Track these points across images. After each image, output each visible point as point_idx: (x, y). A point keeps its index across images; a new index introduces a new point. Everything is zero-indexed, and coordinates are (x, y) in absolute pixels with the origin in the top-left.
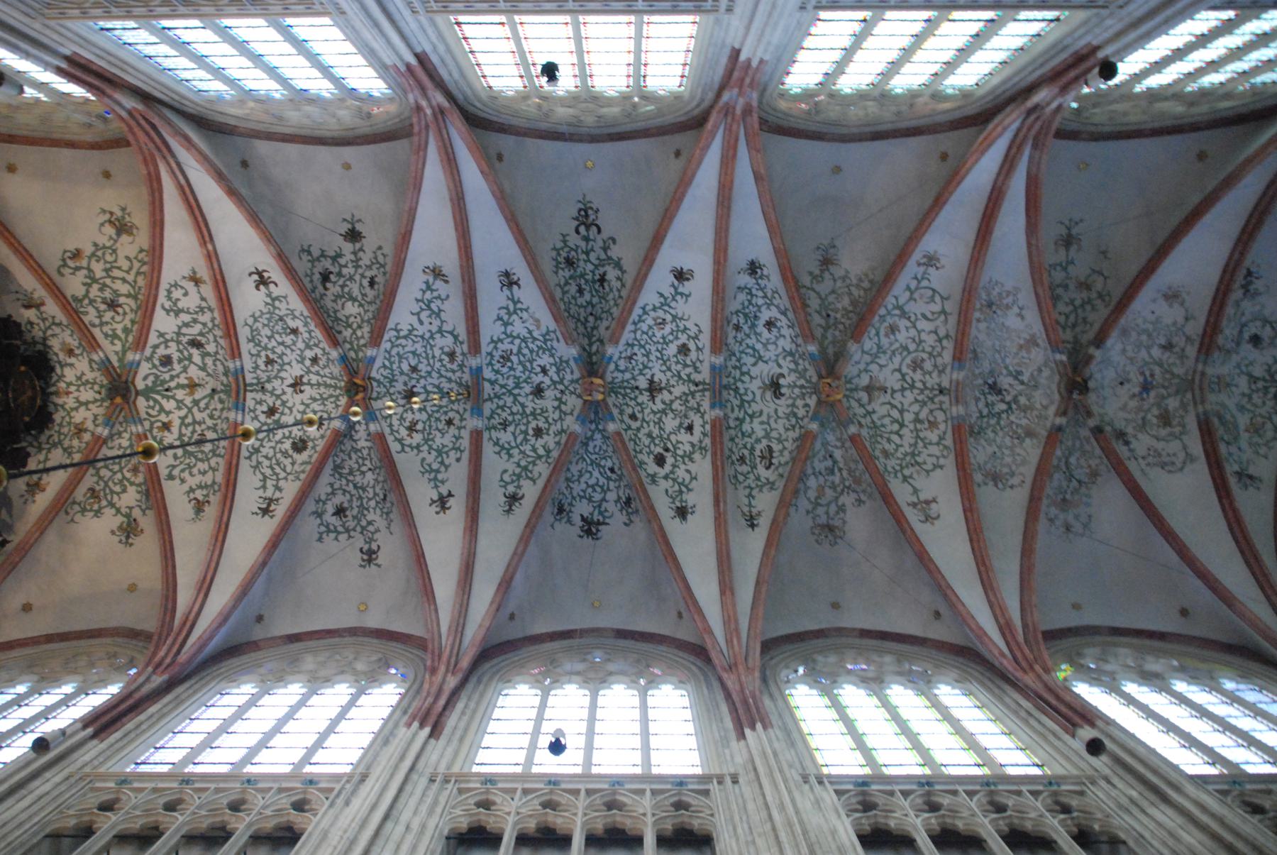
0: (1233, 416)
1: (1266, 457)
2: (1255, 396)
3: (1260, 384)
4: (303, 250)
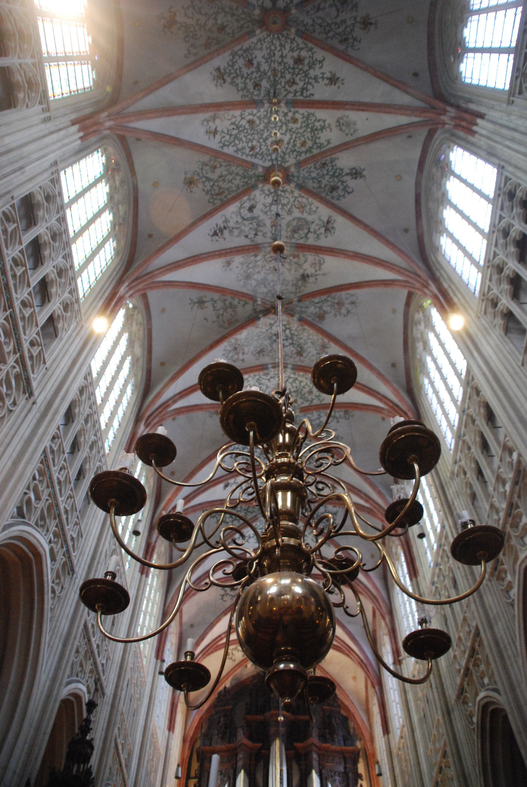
0: (294, 220)
2: (283, 202)
4: (222, 599)
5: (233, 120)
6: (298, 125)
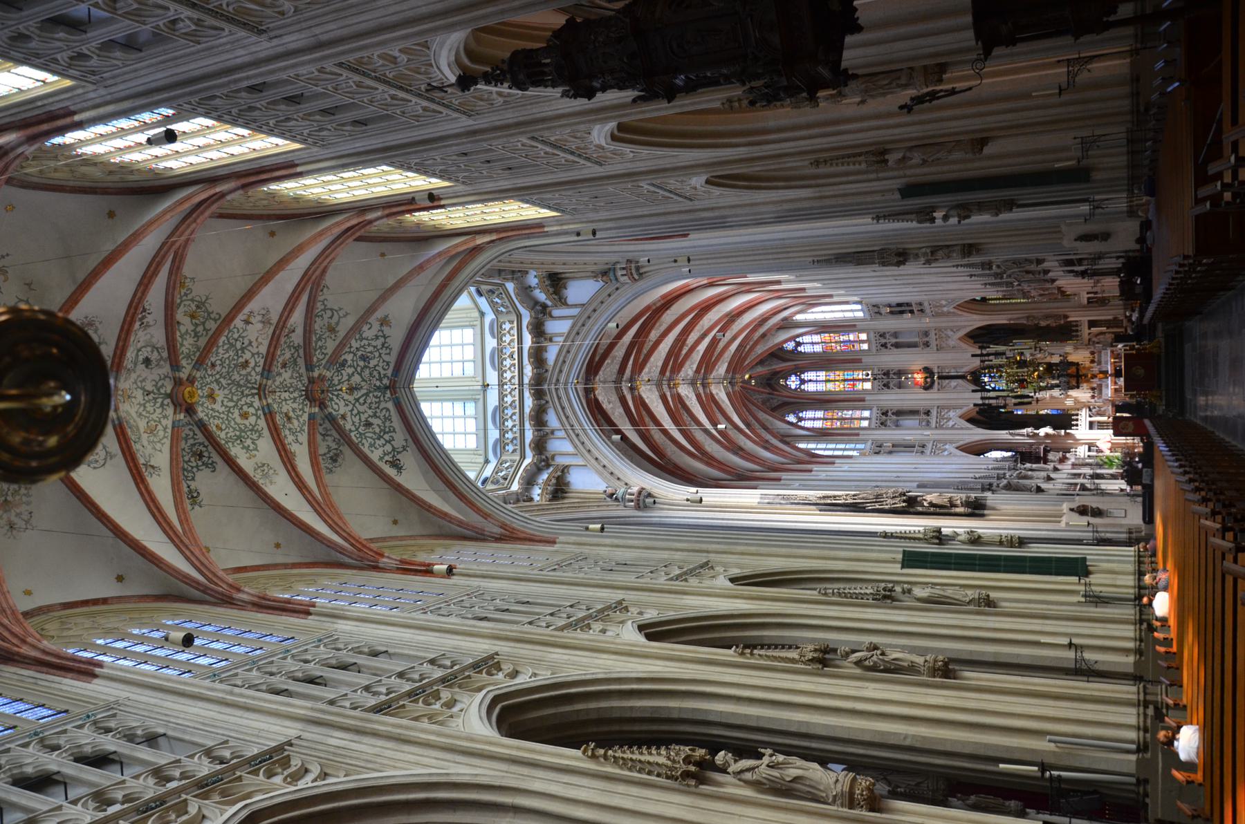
1: (160, 451)
2: (147, 405)
3: (151, 397)
5: (255, 344)
6: (239, 420)
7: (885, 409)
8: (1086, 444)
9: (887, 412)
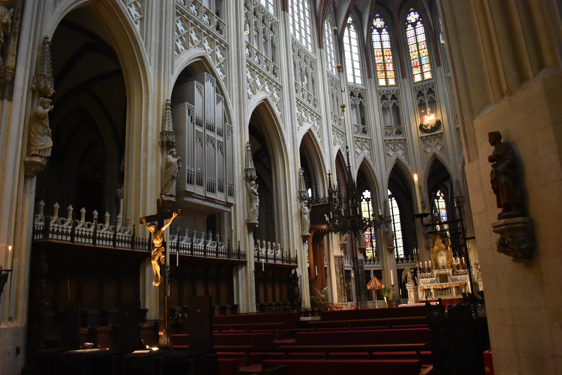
7: (398, 97)
8: (383, 267)
9: (396, 99)
